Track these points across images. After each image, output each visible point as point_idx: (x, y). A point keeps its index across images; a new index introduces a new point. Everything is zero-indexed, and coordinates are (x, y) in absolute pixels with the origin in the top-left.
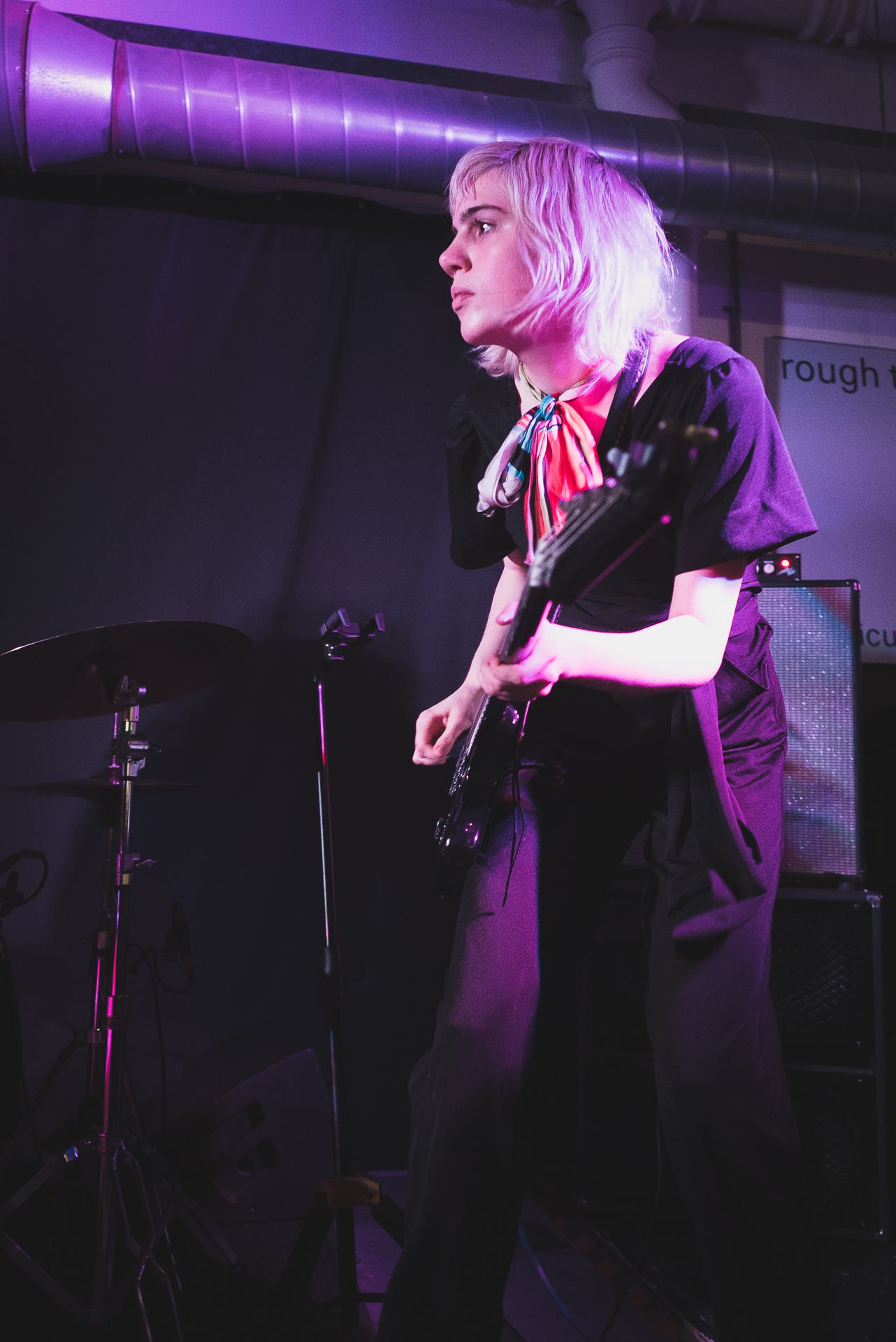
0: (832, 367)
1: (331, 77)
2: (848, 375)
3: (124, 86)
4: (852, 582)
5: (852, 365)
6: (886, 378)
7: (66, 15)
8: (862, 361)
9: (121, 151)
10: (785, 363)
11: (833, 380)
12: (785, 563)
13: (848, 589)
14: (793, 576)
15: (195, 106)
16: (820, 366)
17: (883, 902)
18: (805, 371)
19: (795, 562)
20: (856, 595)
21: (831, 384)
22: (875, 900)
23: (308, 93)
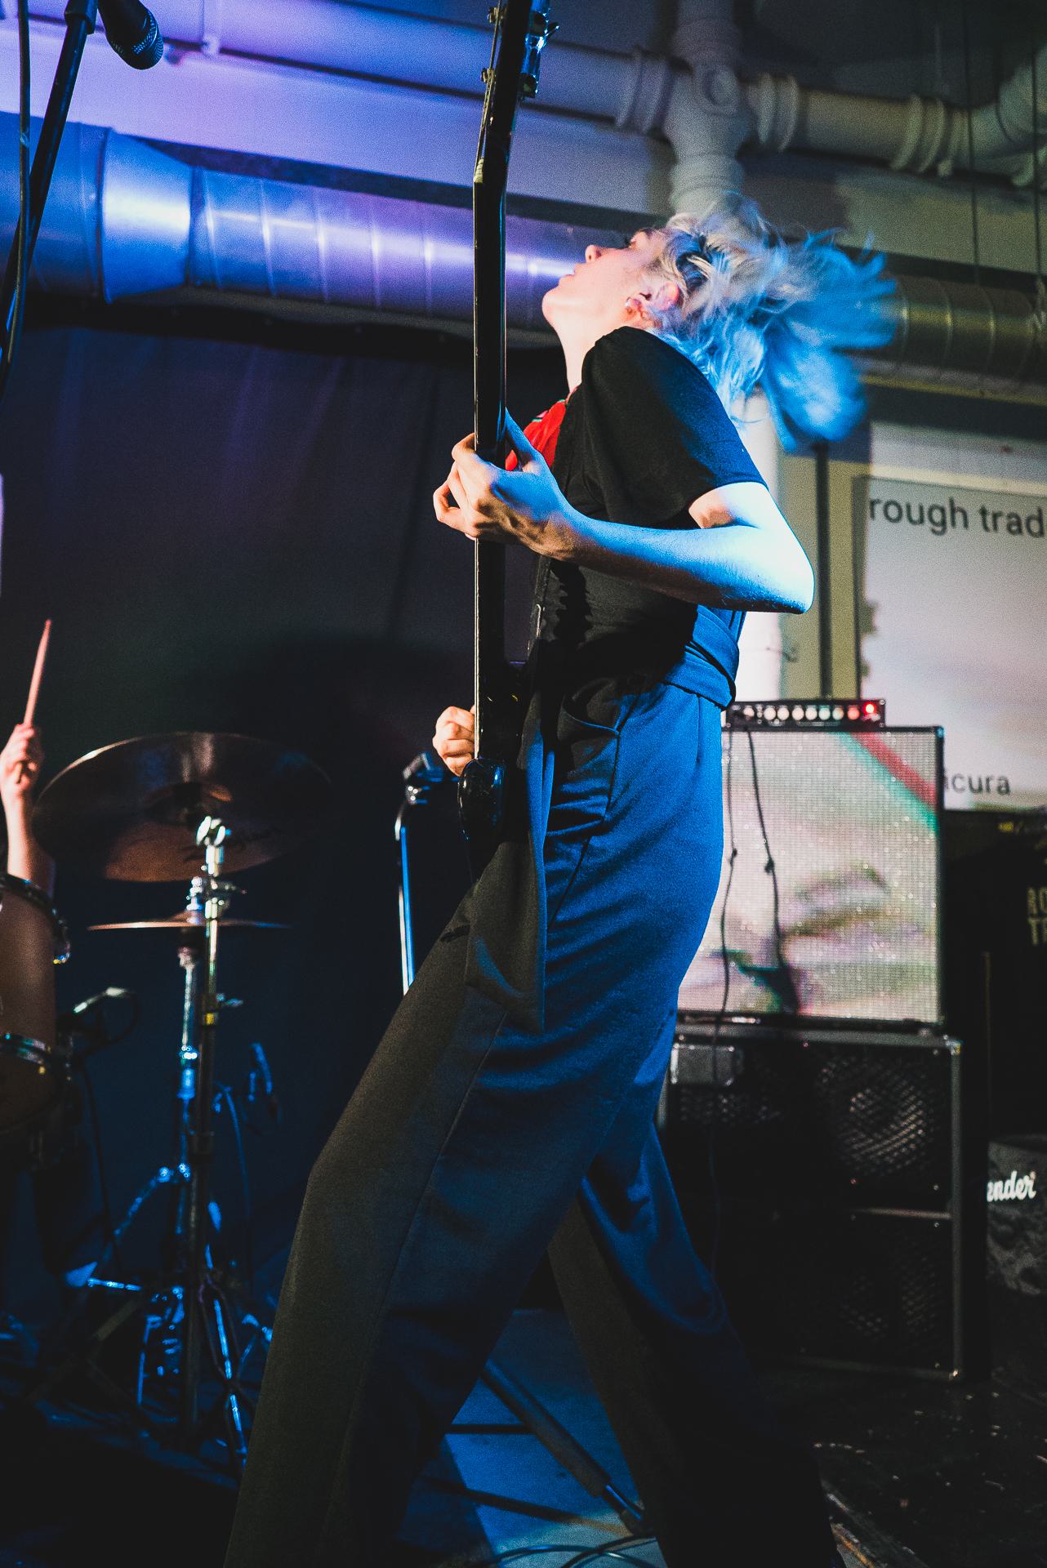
0: (921, 509)
1: (412, 207)
3: (202, 216)
5: (941, 505)
6: (975, 519)
8: (952, 502)
9: (199, 283)
10: (873, 503)
11: (921, 521)
12: (870, 708)
13: (932, 736)
14: (877, 722)
15: (275, 236)
16: (909, 507)
17: (962, 1048)
18: (893, 512)
19: (880, 709)
20: (940, 742)
21: (919, 527)
23: (389, 222)
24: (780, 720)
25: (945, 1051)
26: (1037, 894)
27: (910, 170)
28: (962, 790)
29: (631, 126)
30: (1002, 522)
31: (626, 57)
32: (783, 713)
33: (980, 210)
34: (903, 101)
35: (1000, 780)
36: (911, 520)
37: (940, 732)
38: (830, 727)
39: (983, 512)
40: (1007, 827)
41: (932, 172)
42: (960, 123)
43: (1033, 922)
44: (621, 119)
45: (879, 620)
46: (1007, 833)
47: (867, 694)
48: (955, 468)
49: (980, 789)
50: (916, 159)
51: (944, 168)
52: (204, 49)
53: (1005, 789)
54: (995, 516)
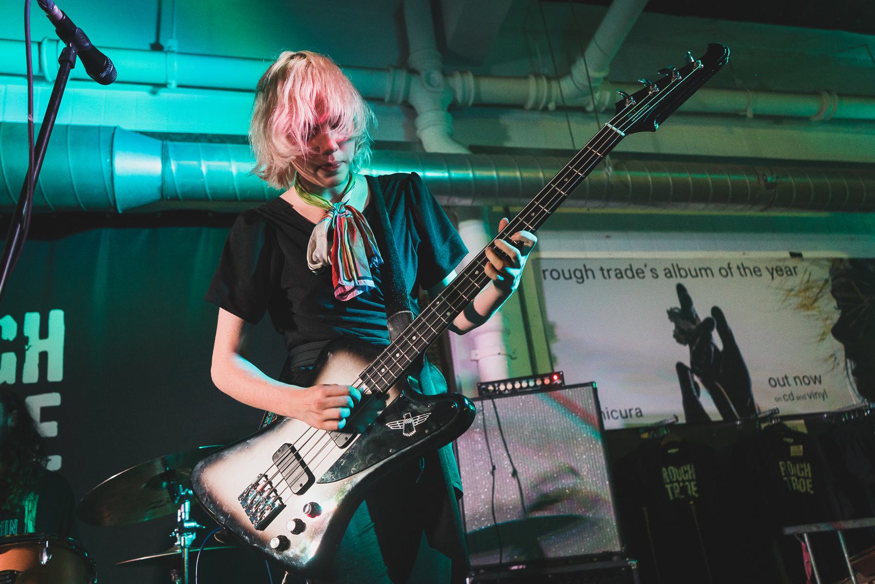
0: (569, 271)
2: (578, 274)
4: (590, 384)
5: (579, 268)
6: (598, 274)
7: (136, 132)
8: (585, 266)
9: (169, 198)
10: (544, 271)
11: (571, 277)
15: (209, 171)
16: (563, 271)
18: (555, 275)
20: (595, 391)
21: (570, 280)
22: (633, 563)
24: (509, 390)
25: (629, 568)
26: (667, 471)
27: (534, 109)
28: (617, 418)
29: (392, 102)
30: (612, 273)
31: (387, 70)
32: (509, 386)
33: (573, 125)
34: (526, 77)
35: (636, 409)
36: (565, 278)
37: (594, 384)
38: (535, 390)
39: (602, 269)
40: (645, 436)
41: (545, 109)
42: (554, 84)
43: (668, 486)
44: (387, 98)
45: (558, 332)
46: (645, 439)
47: (557, 369)
48: (583, 249)
49: (627, 416)
50: (537, 103)
51: (552, 106)
52: (169, 86)
53: (640, 414)
54: (608, 271)
